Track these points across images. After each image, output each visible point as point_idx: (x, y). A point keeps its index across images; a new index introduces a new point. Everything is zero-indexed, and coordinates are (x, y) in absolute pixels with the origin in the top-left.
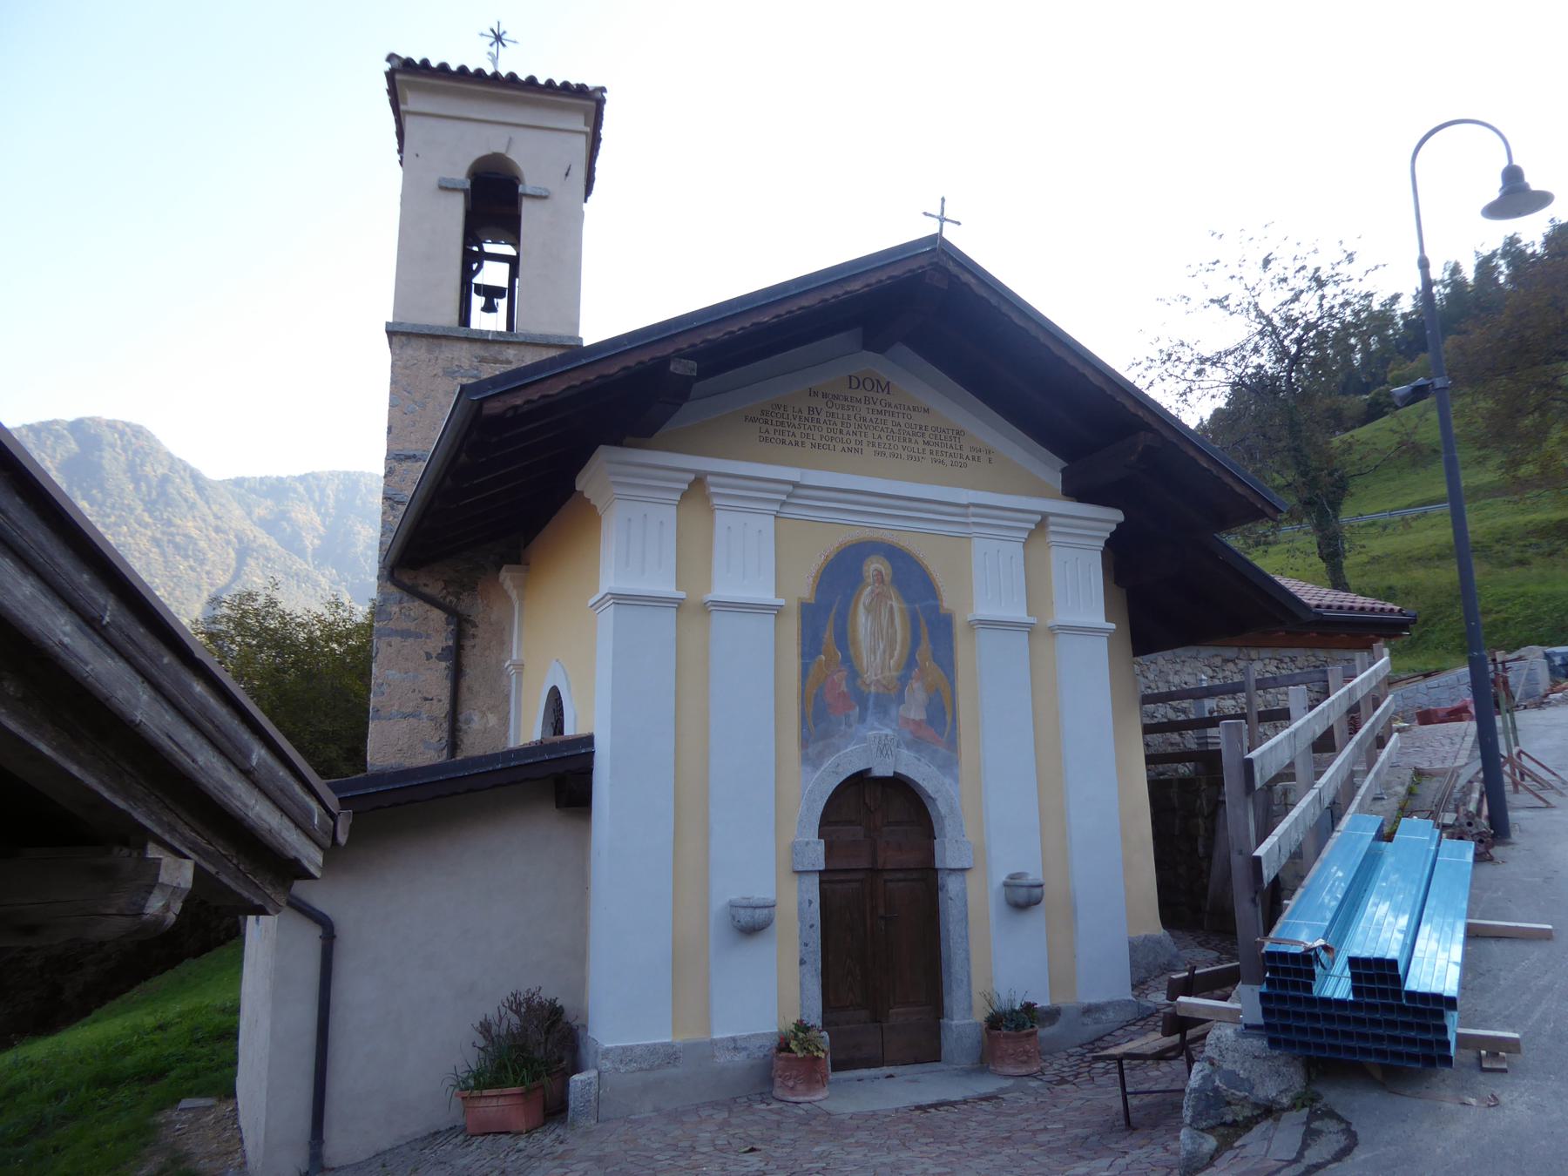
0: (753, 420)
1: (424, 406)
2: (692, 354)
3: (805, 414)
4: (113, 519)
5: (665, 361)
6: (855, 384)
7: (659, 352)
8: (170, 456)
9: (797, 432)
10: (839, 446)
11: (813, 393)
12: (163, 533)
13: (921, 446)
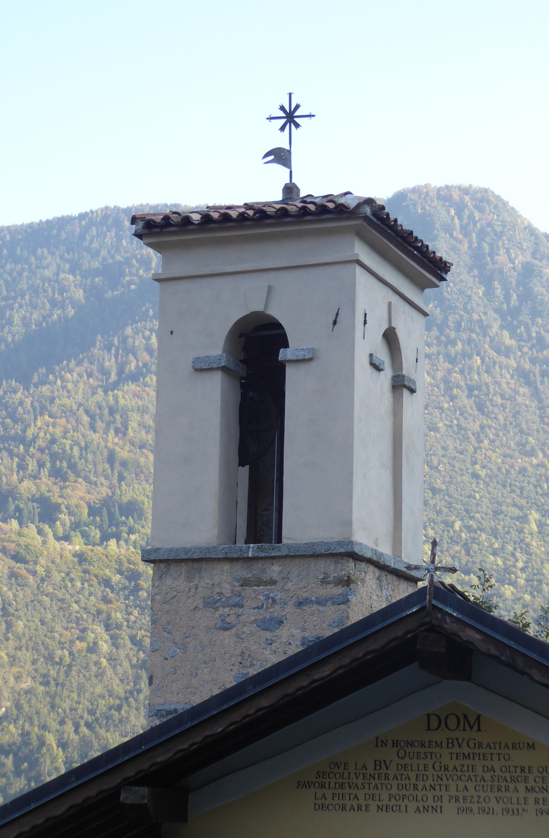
0: (307, 785)
1: (184, 648)
2: (141, 780)
3: (370, 769)
4: (459, 346)
5: (116, 792)
6: (434, 723)
7: (108, 784)
8: (531, 231)
9: (361, 794)
10: (412, 806)
11: (380, 743)
12: (533, 361)
13: (522, 793)
